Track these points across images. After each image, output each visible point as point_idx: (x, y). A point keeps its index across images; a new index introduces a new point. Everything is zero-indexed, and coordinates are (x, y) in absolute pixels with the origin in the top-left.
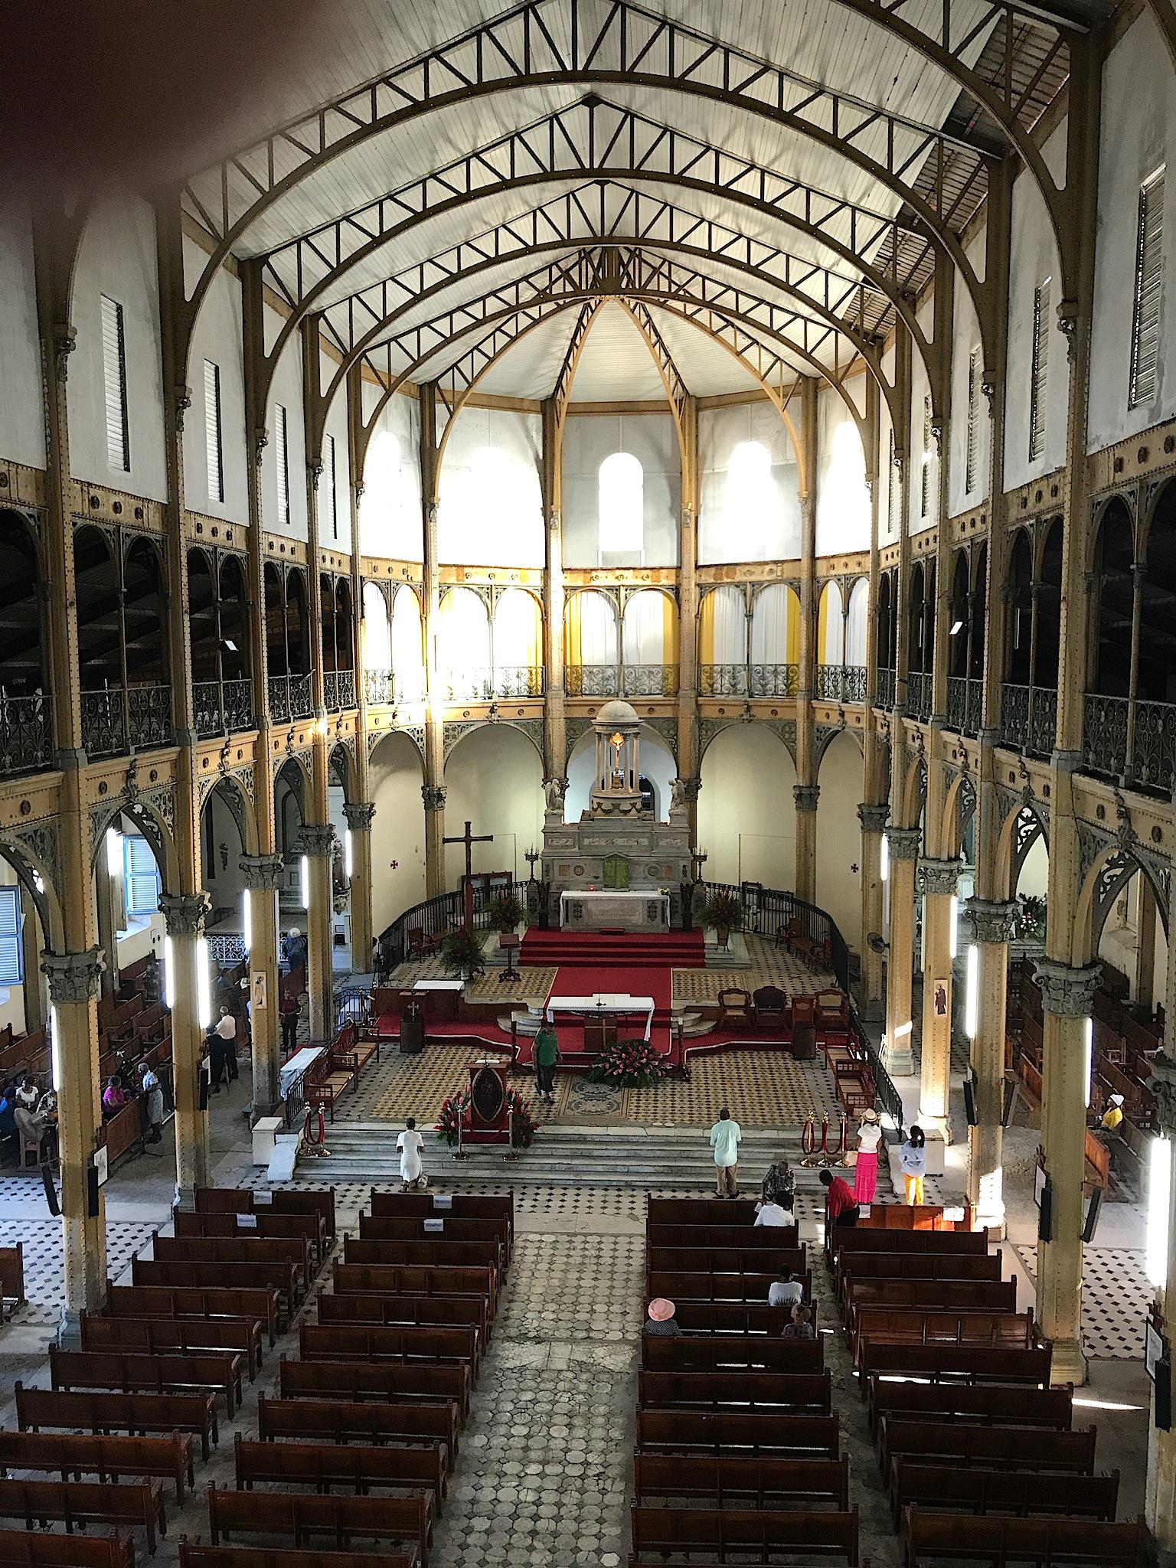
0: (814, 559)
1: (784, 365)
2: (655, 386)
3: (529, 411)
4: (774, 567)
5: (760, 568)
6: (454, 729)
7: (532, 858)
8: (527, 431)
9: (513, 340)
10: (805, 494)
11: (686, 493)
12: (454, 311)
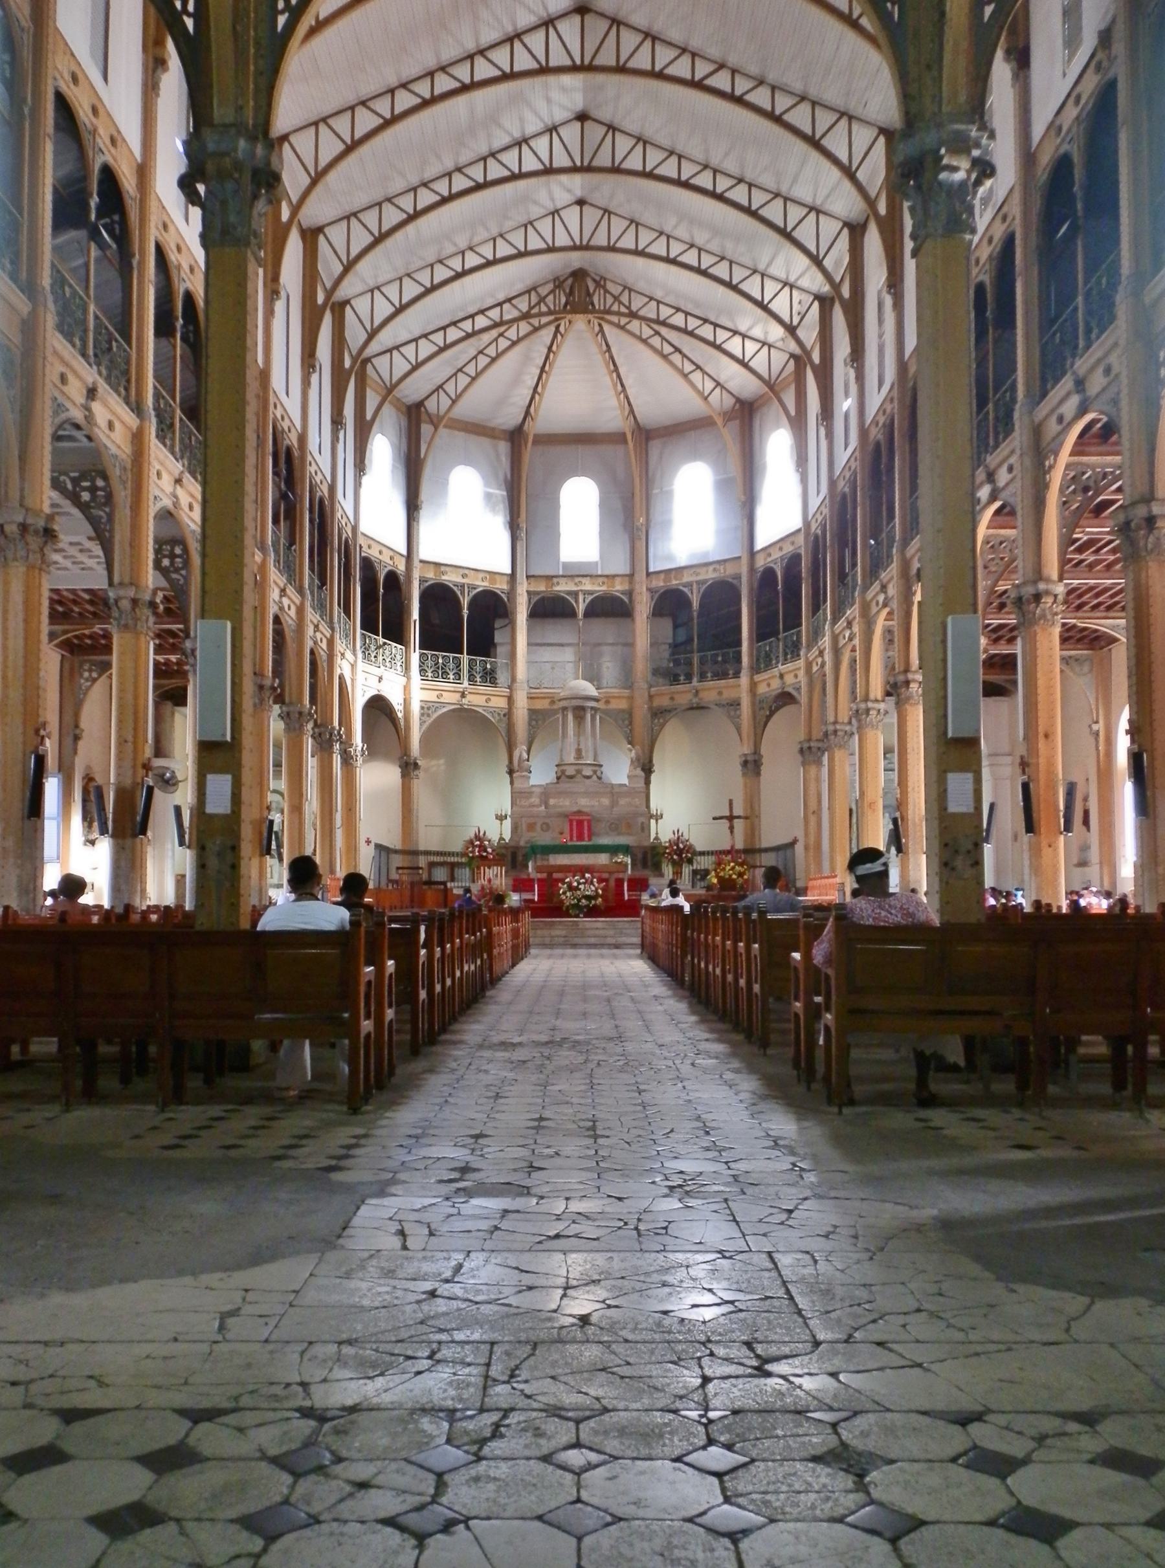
0: (752, 554)
2: (611, 419)
4: (717, 566)
5: (705, 569)
6: (428, 708)
7: (501, 818)
8: (498, 455)
9: (494, 360)
10: (743, 498)
11: (638, 506)
12: (448, 326)
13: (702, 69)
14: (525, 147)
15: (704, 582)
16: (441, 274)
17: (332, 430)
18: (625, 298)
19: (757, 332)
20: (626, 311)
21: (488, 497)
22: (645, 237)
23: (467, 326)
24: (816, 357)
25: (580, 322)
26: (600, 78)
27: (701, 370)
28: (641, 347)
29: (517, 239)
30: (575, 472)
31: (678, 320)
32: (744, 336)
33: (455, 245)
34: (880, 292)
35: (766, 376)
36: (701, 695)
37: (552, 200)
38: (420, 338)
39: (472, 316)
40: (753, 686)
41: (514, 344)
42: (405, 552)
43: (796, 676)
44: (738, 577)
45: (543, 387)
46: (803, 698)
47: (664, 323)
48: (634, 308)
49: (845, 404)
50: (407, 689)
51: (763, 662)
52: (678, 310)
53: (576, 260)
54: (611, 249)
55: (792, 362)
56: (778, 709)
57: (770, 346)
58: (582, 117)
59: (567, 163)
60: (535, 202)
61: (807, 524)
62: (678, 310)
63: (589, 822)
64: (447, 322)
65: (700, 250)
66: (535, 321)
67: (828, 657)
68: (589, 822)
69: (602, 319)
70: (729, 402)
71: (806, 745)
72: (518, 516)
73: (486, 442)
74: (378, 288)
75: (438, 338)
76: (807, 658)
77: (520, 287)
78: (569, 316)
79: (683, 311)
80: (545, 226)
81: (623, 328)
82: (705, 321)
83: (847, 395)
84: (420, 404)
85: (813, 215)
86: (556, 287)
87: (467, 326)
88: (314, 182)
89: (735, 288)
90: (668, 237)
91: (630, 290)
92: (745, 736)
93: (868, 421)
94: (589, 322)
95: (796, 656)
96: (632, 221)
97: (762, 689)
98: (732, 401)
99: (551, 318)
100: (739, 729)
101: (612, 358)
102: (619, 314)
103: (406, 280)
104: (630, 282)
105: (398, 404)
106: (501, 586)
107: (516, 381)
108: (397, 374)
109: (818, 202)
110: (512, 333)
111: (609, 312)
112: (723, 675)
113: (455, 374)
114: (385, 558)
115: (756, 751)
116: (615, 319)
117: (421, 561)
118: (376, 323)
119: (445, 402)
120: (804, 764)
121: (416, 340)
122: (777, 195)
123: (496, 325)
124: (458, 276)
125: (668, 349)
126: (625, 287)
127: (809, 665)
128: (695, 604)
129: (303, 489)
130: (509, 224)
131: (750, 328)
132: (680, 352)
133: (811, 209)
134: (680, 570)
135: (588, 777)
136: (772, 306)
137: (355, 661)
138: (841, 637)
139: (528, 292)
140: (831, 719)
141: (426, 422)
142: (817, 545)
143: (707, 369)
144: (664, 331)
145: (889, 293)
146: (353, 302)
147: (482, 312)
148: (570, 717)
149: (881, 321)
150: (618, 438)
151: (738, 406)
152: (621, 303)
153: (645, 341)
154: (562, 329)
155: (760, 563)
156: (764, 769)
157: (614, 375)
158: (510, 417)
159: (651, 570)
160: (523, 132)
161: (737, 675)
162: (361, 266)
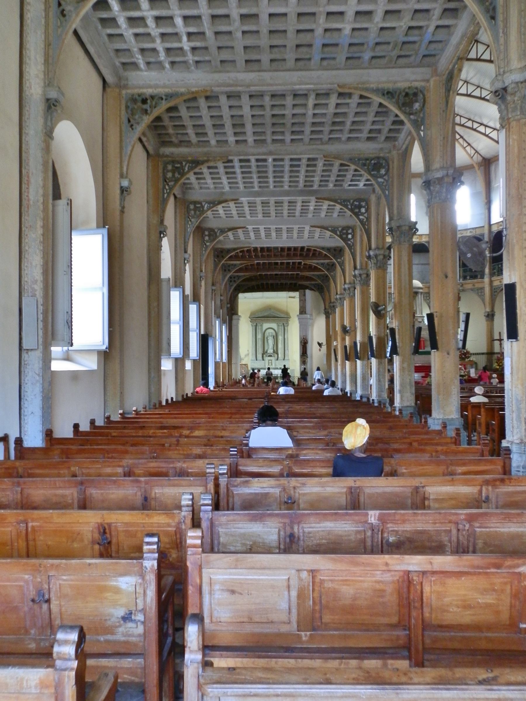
0: (490, 225)
1: (479, 155)
4: (472, 230)
5: (465, 232)
10: (486, 201)
40: (491, 282)
44: (483, 235)
63: (424, 341)
68: (424, 341)
100: (483, 301)
115: (493, 310)
143: (473, 145)
155: (495, 229)
156: (496, 318)
161: (482, 277)
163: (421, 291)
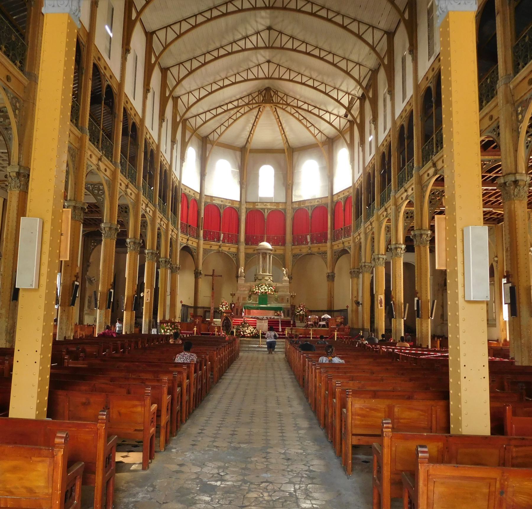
0: (332, 195)
1: (322, 134)
3: (237, 150)
9: (235, 120)
13: (316, 8)
14: (247, 40)
15: (314, 206)
16: (215, 87)
17: (171, 145)
18: (285, 98)
19: (335, 112)
20: (285, 103)
21: (232, 171)
22: (293, 75)
23: (225, 107)
24: (358, 121)
25: (268, 108)
26: (276, 12)
27: (314, 126)
28: (291, 117)
29: (244, 75)
30: (265, 163)
31: (305, 107)
32: (330, 113)
33: (220, 76)
34: (384, 95)
35: (339, 128)
36: (312, 249)
37: (258, 60)
38: (207, 111)
39: (227, 104)
40: (332, 246)
41: (243, 115)
42: (199, 191)
43: (349, 243)
44: (327, 204)
45: (254, 131)
46: (352, 252)
47: (300, 108)
48: (288, 102)
49: (370, 138)
50: (198, 244)
51: (336, 237)
52: (305, 103)
53: (267, 83)
54: (280, 79)
55: (348, 123)
56: (341, 255)
57: (340, 117)
58: (269, 28)
59: (263, 45)
60: (251, 61)
61: (354, 184)
62: (305, 103)
64: (217, 106)
65: (314, 80)
66: (251, 106)
67: (362, 236)
69: (276, 106)
70: (324, 138)
71: (353, 270)
72: (243, 179)
73: (231, 151)
74: (191, 92)
75: (214, 112)
76: (353, 236)
77: (245, 94)
78: (264, 105)
79: (307, 104)
80: (255, 70)
81: (284, 109)
82: (316, 107)
83: (370, 135)
84: (207, 137)
85: (358, 66)
86: (259, 94)
87: (225, 107)
88: (165, 49)
89: (327, 94)
90: (302, 75)
91: (287, 95)
92: (328, 265)
93: (379, 145)
94: (271, 107)
95: (349, 236)
96: (288, 69)
97: (335, 248)
98: (326, 138)
99: (257, 105)
100: (326, 263)
101: (280, 121)
102: (283, 104)
103: (202, 90)
104: (287, 92)
105: (198, 136)
106: (236, 205)
107: (244, 129)
108: (198, 125)
109: (360, 61)
110: (242, 111)
111: (279, 103)
112: (320, 242)
113: (220, 126)
114: (191, 194)
115: (333, 272)
116: (281, 106)
117: (205, 195)
118: (190, 105)
119: (216, 136)
120: (352, 278)
121: (205, 112)
122: (344, 58)
123: (236, 107)
124: (221, 88)
125: (301, 118)
126: (285, 94)
127: (354, 239)
128: (310, 214)
129: (158, 166)
130: (241, 69)
131: (333, 110)
132: (306, 119)
133: (357, 63)
134: (304, 201)
135: (267, 280)
136: (341, 101)
137: (178, 233)
138: (367, 229)
139: (249, 95)
140: (363, 260)
141: (209, 143)
142: (358, 193)
143: (316, 126)
144: (300, 111)
145: (389, 94)
146: (181, 97)
147: (231, 102)
148: (261, 257)
149: (385, 106)
150: (282, 151)
151: (327, 140)
152: (283, 100)
153: (292, 115)
154: (261, 110)
155: (335, 199)
156: (336, 279)
157: (281, 127)
158: (241, 142)
159: (293, 201)
160: (247, 33)
161: (326, 242)
162: (184, 82)
163: (270, 252)
